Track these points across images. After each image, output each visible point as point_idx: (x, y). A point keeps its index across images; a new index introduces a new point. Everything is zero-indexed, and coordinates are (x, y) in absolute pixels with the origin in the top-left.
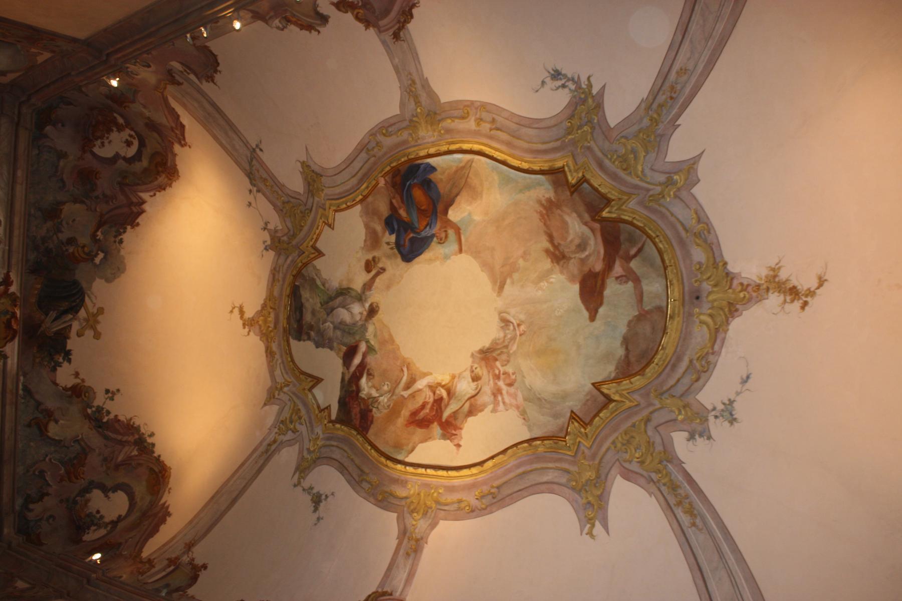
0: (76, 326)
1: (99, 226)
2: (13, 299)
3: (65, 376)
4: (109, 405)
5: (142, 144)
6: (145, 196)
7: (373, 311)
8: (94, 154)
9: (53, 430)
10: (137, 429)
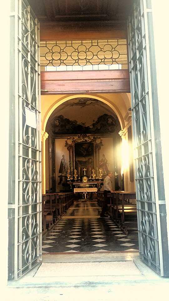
0: (84, 126)
1: (69, 124)
2: (80, 135)
3: (91, 127)
4: (95, 121)
5: (57, 119)
6: (64, 118)
7: (82, 99)
8: (59, 125)
9: (99, 128)
10: (99, 118)
